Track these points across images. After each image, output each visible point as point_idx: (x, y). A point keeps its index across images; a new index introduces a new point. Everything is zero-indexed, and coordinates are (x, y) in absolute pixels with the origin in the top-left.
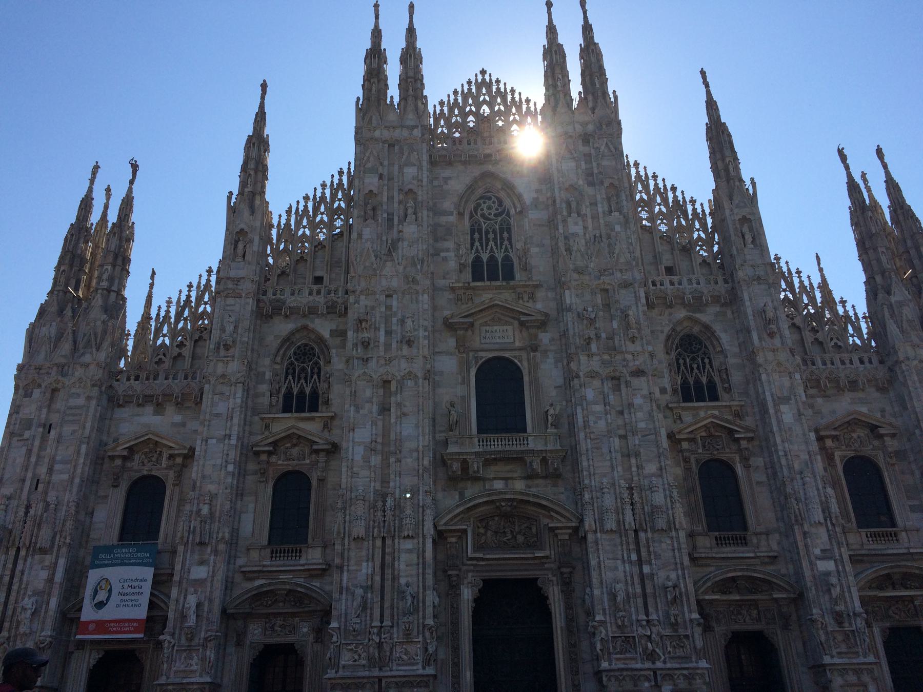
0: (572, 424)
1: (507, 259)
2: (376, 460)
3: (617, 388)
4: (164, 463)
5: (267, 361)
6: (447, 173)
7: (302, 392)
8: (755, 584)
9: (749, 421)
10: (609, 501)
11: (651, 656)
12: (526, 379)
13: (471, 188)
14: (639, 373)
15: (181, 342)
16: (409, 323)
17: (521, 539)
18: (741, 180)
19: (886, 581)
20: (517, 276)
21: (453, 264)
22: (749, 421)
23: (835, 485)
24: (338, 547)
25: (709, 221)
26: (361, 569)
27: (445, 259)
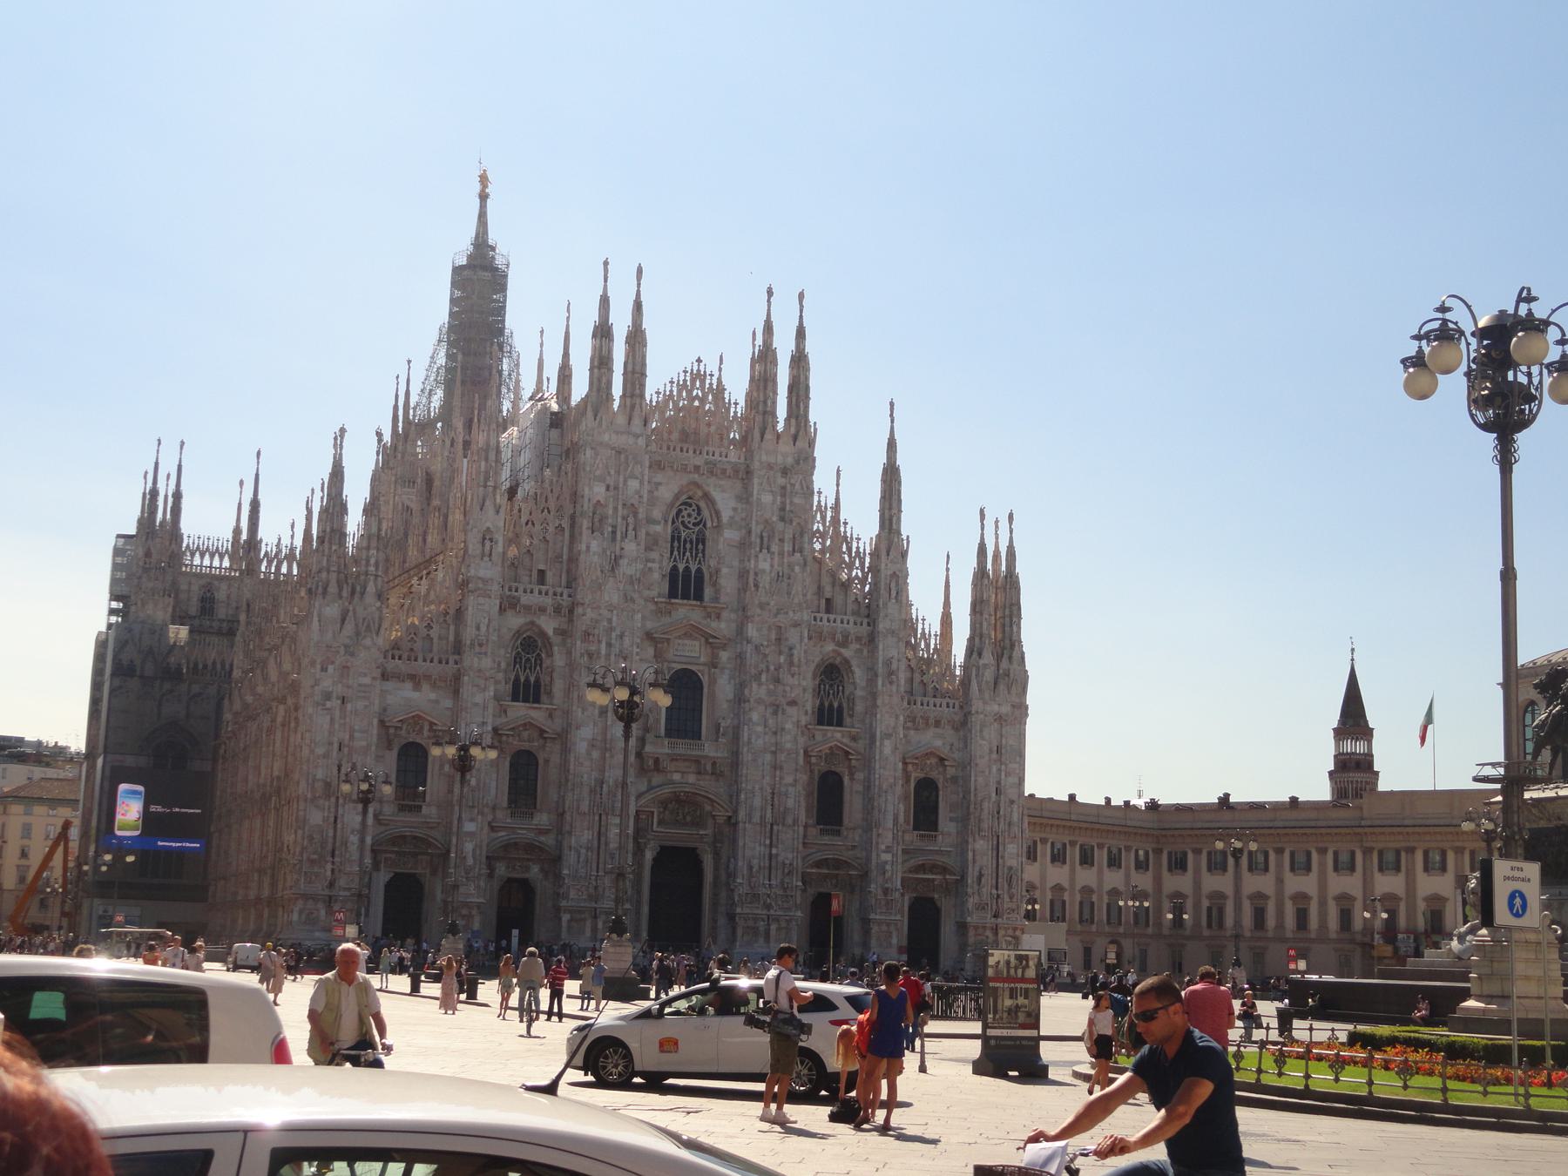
0: (736, 737)
1: (699, 571)
2: (596, 754)
3: (775, 713)
4: (426, 733)
5: (502, 652)
6: (659, 477)
7: (527, 680)
8: (838, 864)
9: (860, 745)
10: (757, 802)
11: (769, 907)
12: (705, 690)
13: (677, 497)
14: (793, 703)
15: (429, 627)
16: (627, 641)
17: (688, 819)
18: (899, 533)
19: (921, 868)
20: (708, 592)
21: (656, 576)
22: (860, 745)
23: (906, 797)
24: (568, 817)
25: (868, 560)
26: (582, 836)
27: (650, 569)
